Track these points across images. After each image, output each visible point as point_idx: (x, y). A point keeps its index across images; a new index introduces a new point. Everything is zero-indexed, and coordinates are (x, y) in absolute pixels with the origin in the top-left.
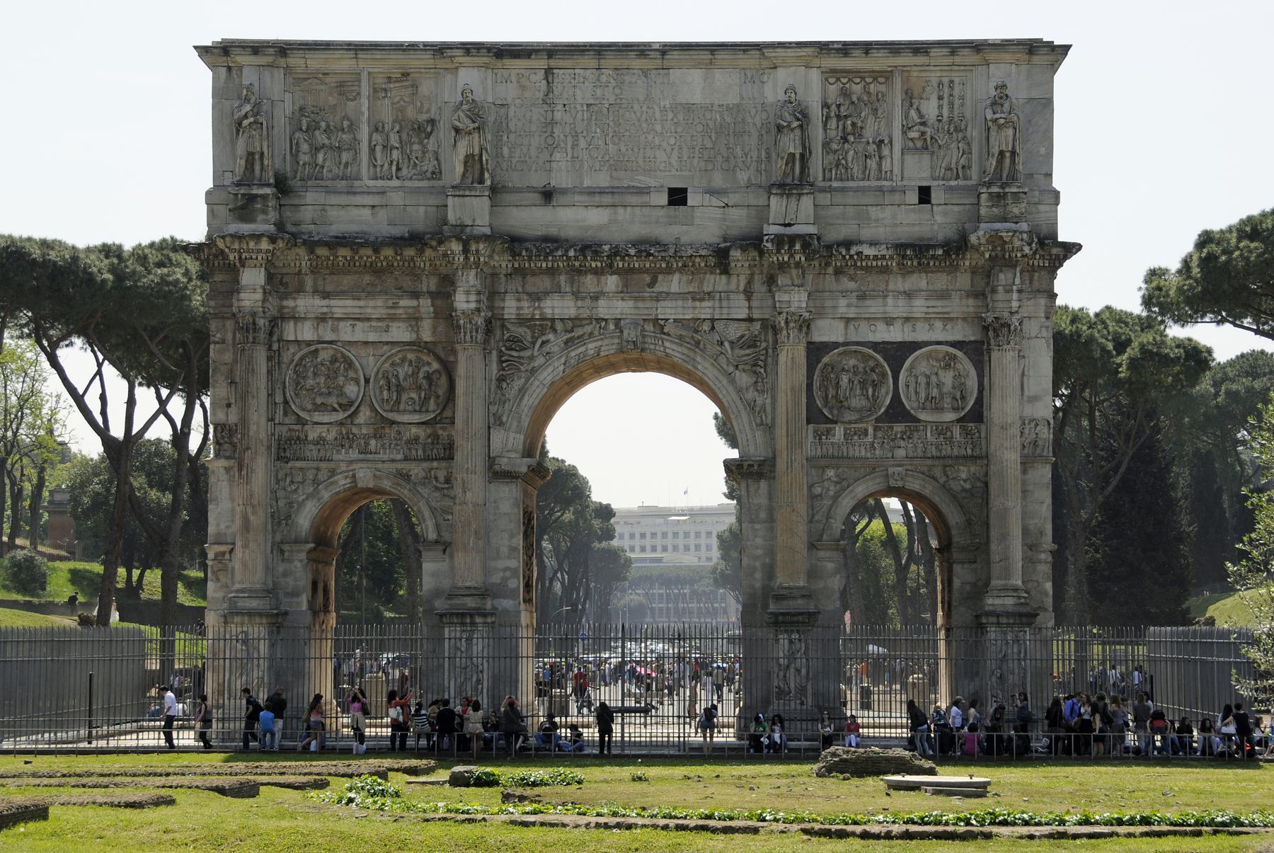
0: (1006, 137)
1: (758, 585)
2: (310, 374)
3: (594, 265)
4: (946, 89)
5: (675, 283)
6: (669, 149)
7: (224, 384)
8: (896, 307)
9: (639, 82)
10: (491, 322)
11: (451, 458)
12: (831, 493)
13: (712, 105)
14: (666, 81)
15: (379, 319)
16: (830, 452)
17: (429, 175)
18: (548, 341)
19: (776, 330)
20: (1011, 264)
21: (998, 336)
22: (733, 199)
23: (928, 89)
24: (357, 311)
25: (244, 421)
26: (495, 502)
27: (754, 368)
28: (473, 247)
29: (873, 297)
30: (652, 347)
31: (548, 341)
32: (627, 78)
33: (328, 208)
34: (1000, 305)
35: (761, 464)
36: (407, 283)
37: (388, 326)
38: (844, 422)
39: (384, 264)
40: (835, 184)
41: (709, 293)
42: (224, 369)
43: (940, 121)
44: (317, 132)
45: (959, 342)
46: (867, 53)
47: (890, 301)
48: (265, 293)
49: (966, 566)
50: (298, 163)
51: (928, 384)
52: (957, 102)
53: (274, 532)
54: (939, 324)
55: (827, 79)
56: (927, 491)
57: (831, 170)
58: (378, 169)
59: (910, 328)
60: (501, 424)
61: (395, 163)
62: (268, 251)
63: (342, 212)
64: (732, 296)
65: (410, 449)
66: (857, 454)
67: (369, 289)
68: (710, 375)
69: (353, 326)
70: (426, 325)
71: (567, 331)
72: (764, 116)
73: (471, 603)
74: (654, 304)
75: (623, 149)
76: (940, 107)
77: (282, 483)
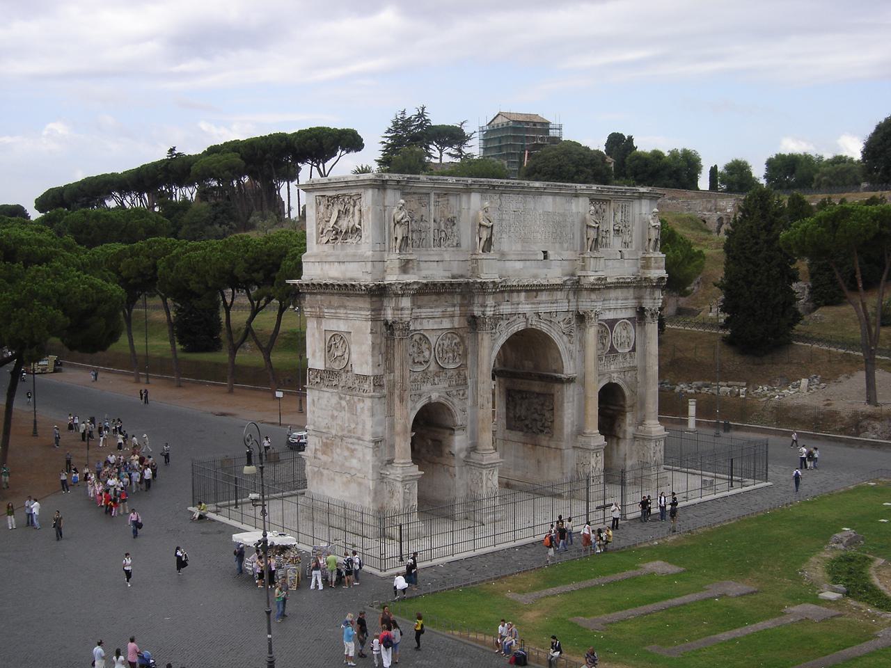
1: (569, 430)
5: (544, 297)
7: (377, 355)
8: (612, 304)
17: (455, 244)
19: (581, 318)
24: (431, 314)
29: (607, 300)
32: (528, 199)
34: (656, 305)
36: (449, 298)
41: (556, 300)
42: (377, 347)
47: (611, 302)
67: (435, 303)
69: (428, 321)
70: (456, 319)
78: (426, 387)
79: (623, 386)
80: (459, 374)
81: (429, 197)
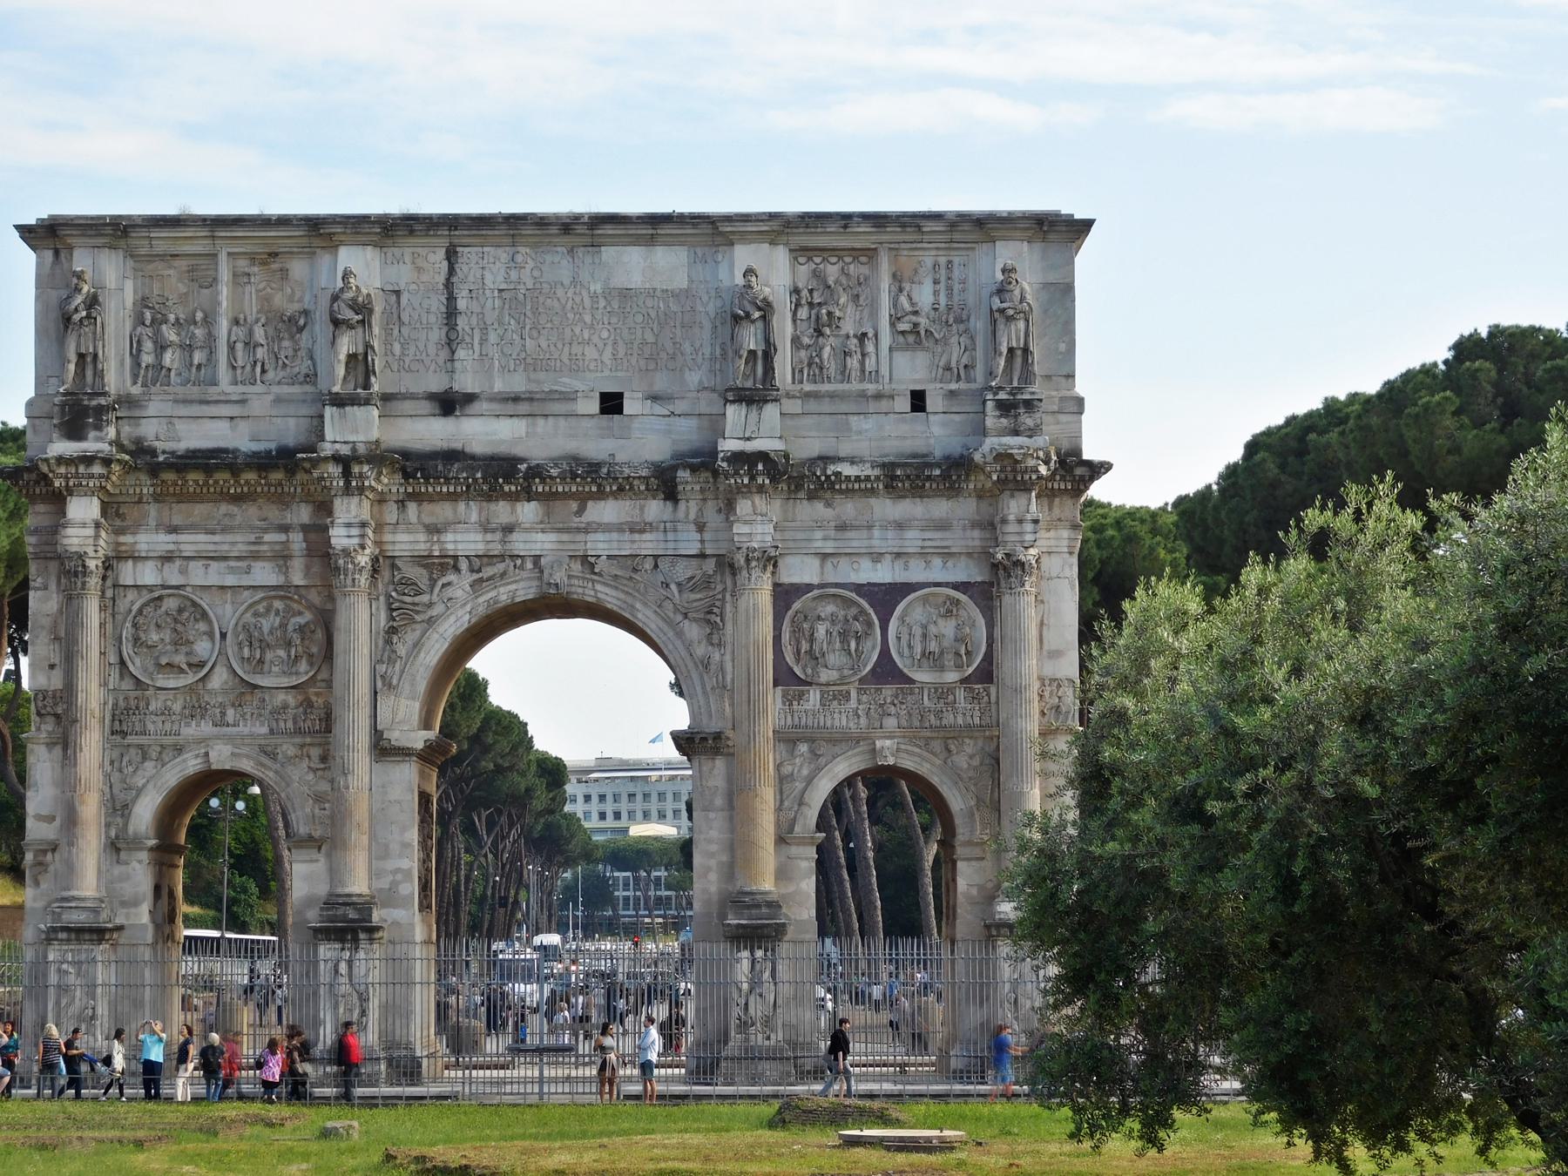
0: (1017, 331)
1: (713, 889)
2: (152, 627)
3: (506, 488)
4: (943, 271)
5: (606, 511)
6: (601, 345)
7: (46, 641)
8: (881, 540)
9: (564, 262)
10: (378, 560)
11: (329, 730)
12: (805, 772)
13: (655, 290)
14: (597, 261)
15: (238, 558)
16: (803, 723)
17: (302, 379)
18: (449, 584)
19: (734, 570)
20: (1025, 487)
21: (1009, 576)
22: (680, 407)
23: (921, 271)
24: (211, 547)
25: (69, 689)
26: (383, 787)
27: (708, 617)
28: (356, 469)
30: (580, 590)
31: (449, 584)
32: (548, 258)
33: (176, 421)
35: (718, 736)
36: (273, 513)
37: (249, 567)
38: (817, 684)
39: (245, 489)
40: (808, 387)
42: (46, 622)
43: (936, 309)
44: (164, 327)
45: (963, 583)
46: (845, 227)
47: (876, 533)
48: (97, 525)
49: (974, 863)
50: (139, 365)
51: (924, 636)
52: (957, 287)
53: (108, 825)
54: (937, 562)
55: (796, 259)
56: (924, 770)
57: (801, 371)
58: (239, 371)
59: (902, 566)
60: (390, 686)
61: (259, 365)
62: (101, 476)
63: (194, 426)
64: (680, 526)
65: (277, 720)
66: (837, 723)
68: (653, 626)
69: (207, 567)
71: (472, 571)
72: (719, 303)
73: (352, 915)
74: (580, 537)
75: (544, 344)
76: (936, 293)
77: (116, 764)
78: (191, 731)
79: (935, 780)
80: (308, 704)
81: (217, 264)
